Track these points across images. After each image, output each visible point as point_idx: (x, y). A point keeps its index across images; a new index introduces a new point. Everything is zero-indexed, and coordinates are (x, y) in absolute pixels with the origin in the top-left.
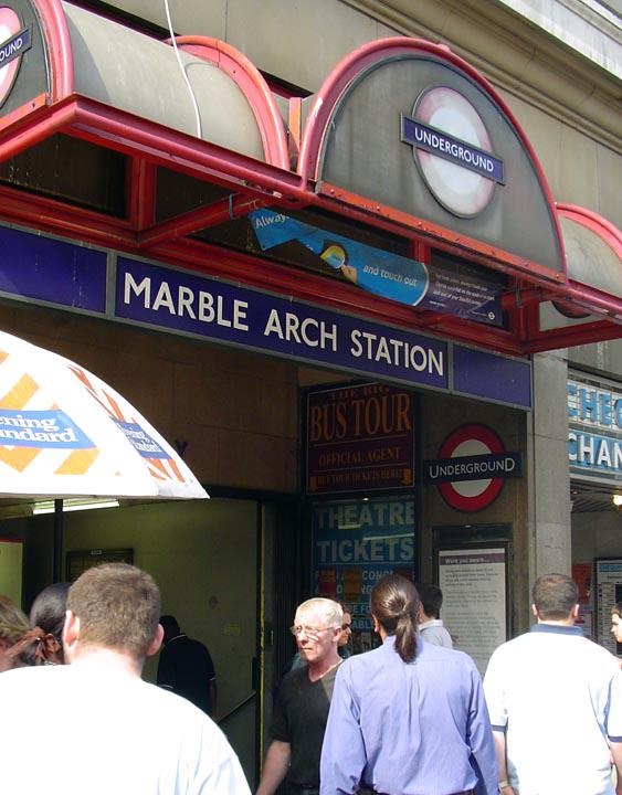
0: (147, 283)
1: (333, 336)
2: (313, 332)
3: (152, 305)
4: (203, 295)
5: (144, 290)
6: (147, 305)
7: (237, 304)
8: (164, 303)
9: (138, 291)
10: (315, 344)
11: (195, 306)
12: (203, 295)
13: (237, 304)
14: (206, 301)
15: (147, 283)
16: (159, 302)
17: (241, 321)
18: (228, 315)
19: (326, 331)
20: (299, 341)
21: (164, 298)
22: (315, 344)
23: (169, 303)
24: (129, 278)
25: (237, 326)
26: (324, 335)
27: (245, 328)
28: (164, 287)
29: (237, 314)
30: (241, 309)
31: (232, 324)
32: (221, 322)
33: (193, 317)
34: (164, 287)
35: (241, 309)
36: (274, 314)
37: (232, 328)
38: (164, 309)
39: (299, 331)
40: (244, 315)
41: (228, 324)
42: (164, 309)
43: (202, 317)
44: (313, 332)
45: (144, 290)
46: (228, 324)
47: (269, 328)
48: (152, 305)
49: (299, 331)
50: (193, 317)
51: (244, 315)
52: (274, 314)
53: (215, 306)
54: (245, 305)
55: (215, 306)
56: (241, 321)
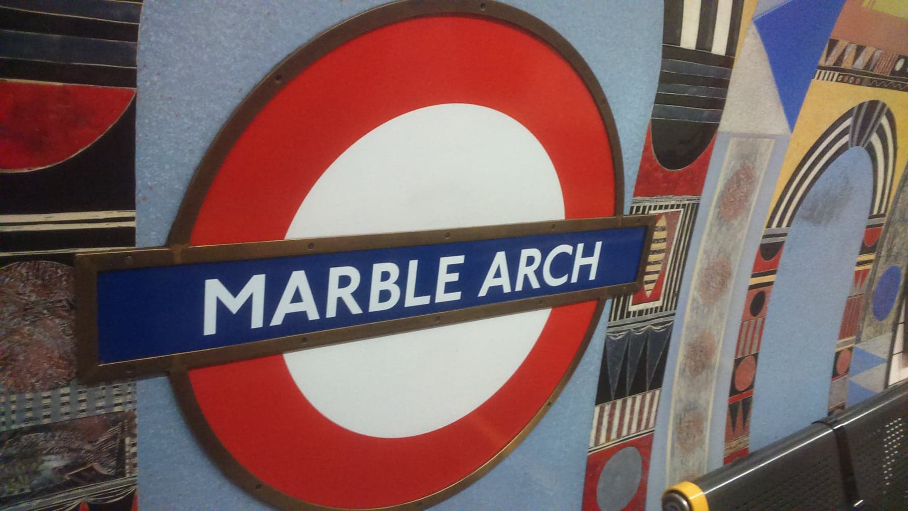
0: (256, 285)
1: (594, 261)
2: (562, 265)
6: (257, 321)
8: (297, 308)
9: (234, 304)
10: (563, 280)
11: (362, 295)
13: (445, 262)
14: (385, 276)
15: (256, 285)
16: (285, 307)
17: (450, 287)
18: (426, 284)
20: (535, 284)
21: (297, 298)
22: (563, 280)
24: (214, 290)
25: (442, 297)
26: (579, 261)
27: (456, 296)
28: (298, 280)
29: (444, 277)
30: (451, 269)
32: (412, 301)
33: (355, 309)
34: (298, 280)
35: (451, 269)
36: (500, 259)
37: (433, 307)
38: (296, 321)
39: (539, 273)
40: (455, 277)
41: (425, 300)
42: (289, 317)
43: (375, 306)
44: (562, 265)
45: (251, 297)
46: (425, 300)
47: (490, 281)
49: (539, 273)
50: (355, 309)
51: (455, 277)
52: (500, 259)
53: (402, 282)
54: (460, 259)
55: (402, 282)
56: (450, 287)
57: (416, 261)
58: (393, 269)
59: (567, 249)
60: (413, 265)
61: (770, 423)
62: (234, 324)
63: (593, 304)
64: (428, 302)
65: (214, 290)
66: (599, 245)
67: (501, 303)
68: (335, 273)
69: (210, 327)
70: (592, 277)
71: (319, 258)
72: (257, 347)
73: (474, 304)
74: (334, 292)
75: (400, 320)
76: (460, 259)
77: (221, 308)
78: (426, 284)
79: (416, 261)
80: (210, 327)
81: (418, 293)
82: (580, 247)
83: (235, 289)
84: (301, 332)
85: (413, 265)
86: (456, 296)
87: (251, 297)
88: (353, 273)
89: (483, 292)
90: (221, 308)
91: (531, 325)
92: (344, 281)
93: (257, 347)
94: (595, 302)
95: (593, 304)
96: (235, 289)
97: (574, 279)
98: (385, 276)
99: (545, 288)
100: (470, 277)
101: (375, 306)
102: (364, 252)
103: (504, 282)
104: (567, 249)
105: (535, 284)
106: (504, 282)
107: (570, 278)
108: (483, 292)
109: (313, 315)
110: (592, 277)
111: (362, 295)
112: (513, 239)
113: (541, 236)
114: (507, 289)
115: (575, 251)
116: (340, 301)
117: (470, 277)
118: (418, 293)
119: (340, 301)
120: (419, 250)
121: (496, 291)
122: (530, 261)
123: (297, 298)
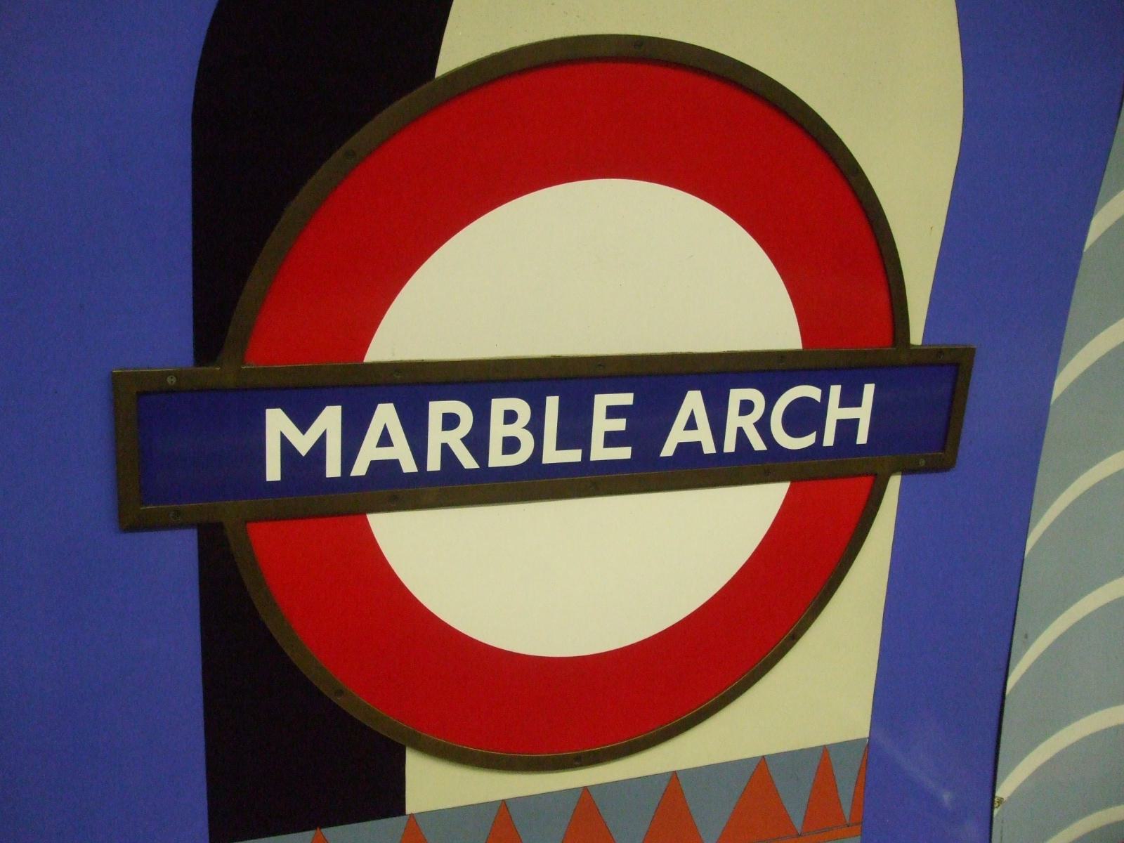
0: (330, 419)
1: (863, 414)
2: (805, 417)
3: (349, 457)
4: (499, 406)
5: (322, 441)
6: (333, 469)
7: (602, 402)
8: (385, 454)
9: (303, 443)
10: (809, 440)
11: (477, 441)
12: (499, 406)
13: (602, 402)
14: (510, 417)
15: (330, 419)
16: (369, 452)
17: (612, 439)
18: (575, 431)
19: (844, 403)
20: (758, 444)
21: (385, 440)
22: (809, 440)
23: (401, 451)
24: (277, 422)
25: (599, 452)
26: (835, 413)
27: (624, 453)
28: (386, 415)
29: (601, 425)
30: (613, 412)
31: (586, 454)
32: (552, 455)
33: (468, 461)
34: (386, 415)
35: (613, 412)
36: (694, 402)
38: (384, 470)
39: (763, 425)
40: (620, 424)
41: (574, 456)
42: (375, 466)
43: (497, 458)
44: (805, 417)
45: (323, 438)
46: (574, 456)
47: (677, 435)
48: (349, 457)
49: (763, 425)
50: (468, 461)
51: (620, 424)
52: (694, 402)
53: (536, 426)
54: (626, 399)
55: (536, 426)
56: (612, 439)
57: (557, 398)
58: (523, 408)
59: (814, 393)
60: (552, 404)
61: (411, 543)
62: (303, 467)
63: (867, 481)
64: (579, 460)
65: (277, 422)
66: (869, 390)
67: (695, 470)
68: (437, 409)
69: (273, 472)
70: (862, 438)
71: (415, 386)
72: (337, 506)
73: (649, 470)
74: (436, 437)
75: (534, 482)
76: (626, 399)
77: (287, 447)
78: (575, 431)
79: (557, 398)
80: (273, 472)
81: (562, 445)
82: (835, 391)
83: (303, 425)
84: (391, 488)
85: (552, 404)
86: (624, 453)
87: (323, 438)
88: (464, 411)
89: (668, 450)
90: (287, 447)
92: (450, 422)
93: (337, 506)
94: (870, 479)
95: (867, 481)
96: (303, 425)
97: (829, 441)
98: (510, 417)
100: (647, 424)
101: (497, 458)
102: (478, 382)
103: (704, 436)
104: (814, 393)
105: (758, 444)
106: (704, 436)
107: (820, 438)
108: (668, 450)
109: (409, 466)
110: (862, 438)
111: (477, 441)
112: (717, 374)
113: (768, 371)
114: (709, 448)
115: (825, 396)
116: (446, 449)
117: (647, 424)
118: (562, 445)
119: (446, 449)
120: (566, 382)
121: (689, 451)
122: (746, 407)
123: (385, 440)
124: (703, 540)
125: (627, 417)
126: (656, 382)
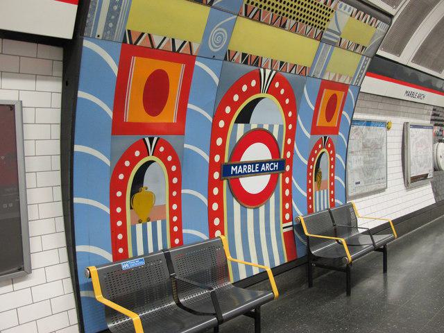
1: (277, 166)
2: (272, 166)
11: (247, 170)
16: (239, 171)
18: (254, 169)
23: (241, 171)
25: (256, 171)
28: (240, 167)
29: (257, 168)
34: (240, 167)
44: (272, 166)
62: (234, 172)
71: (242, 164)
73: (260, 172)
74: (244, 169)
75: (251, 174)
78: (254, 169)
91: (267, 178)
99: (270, 171)
100: (260, 168)
102: (247, 164)
111: (247, 170)
112: (265, 162)
113: (269, 162)
117: (260, 168)
120: (253, 163)
124: (264, 180)
125: (258, 167)
126: (261, 163)
